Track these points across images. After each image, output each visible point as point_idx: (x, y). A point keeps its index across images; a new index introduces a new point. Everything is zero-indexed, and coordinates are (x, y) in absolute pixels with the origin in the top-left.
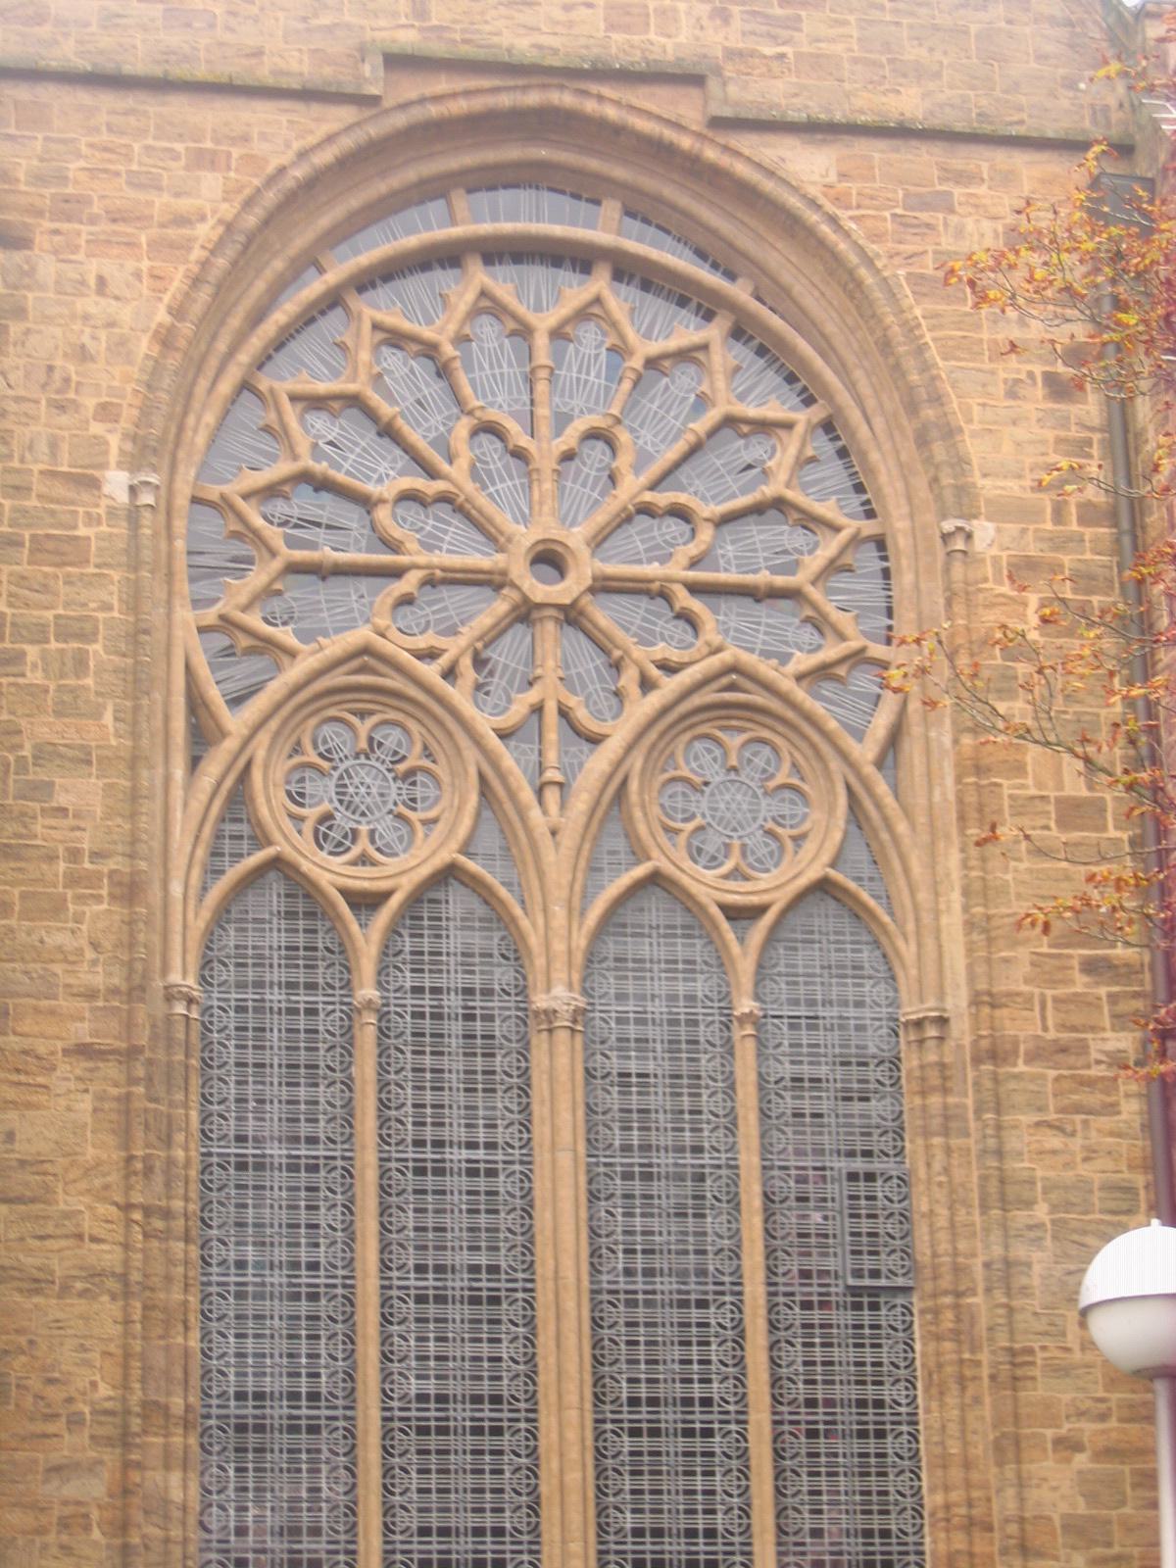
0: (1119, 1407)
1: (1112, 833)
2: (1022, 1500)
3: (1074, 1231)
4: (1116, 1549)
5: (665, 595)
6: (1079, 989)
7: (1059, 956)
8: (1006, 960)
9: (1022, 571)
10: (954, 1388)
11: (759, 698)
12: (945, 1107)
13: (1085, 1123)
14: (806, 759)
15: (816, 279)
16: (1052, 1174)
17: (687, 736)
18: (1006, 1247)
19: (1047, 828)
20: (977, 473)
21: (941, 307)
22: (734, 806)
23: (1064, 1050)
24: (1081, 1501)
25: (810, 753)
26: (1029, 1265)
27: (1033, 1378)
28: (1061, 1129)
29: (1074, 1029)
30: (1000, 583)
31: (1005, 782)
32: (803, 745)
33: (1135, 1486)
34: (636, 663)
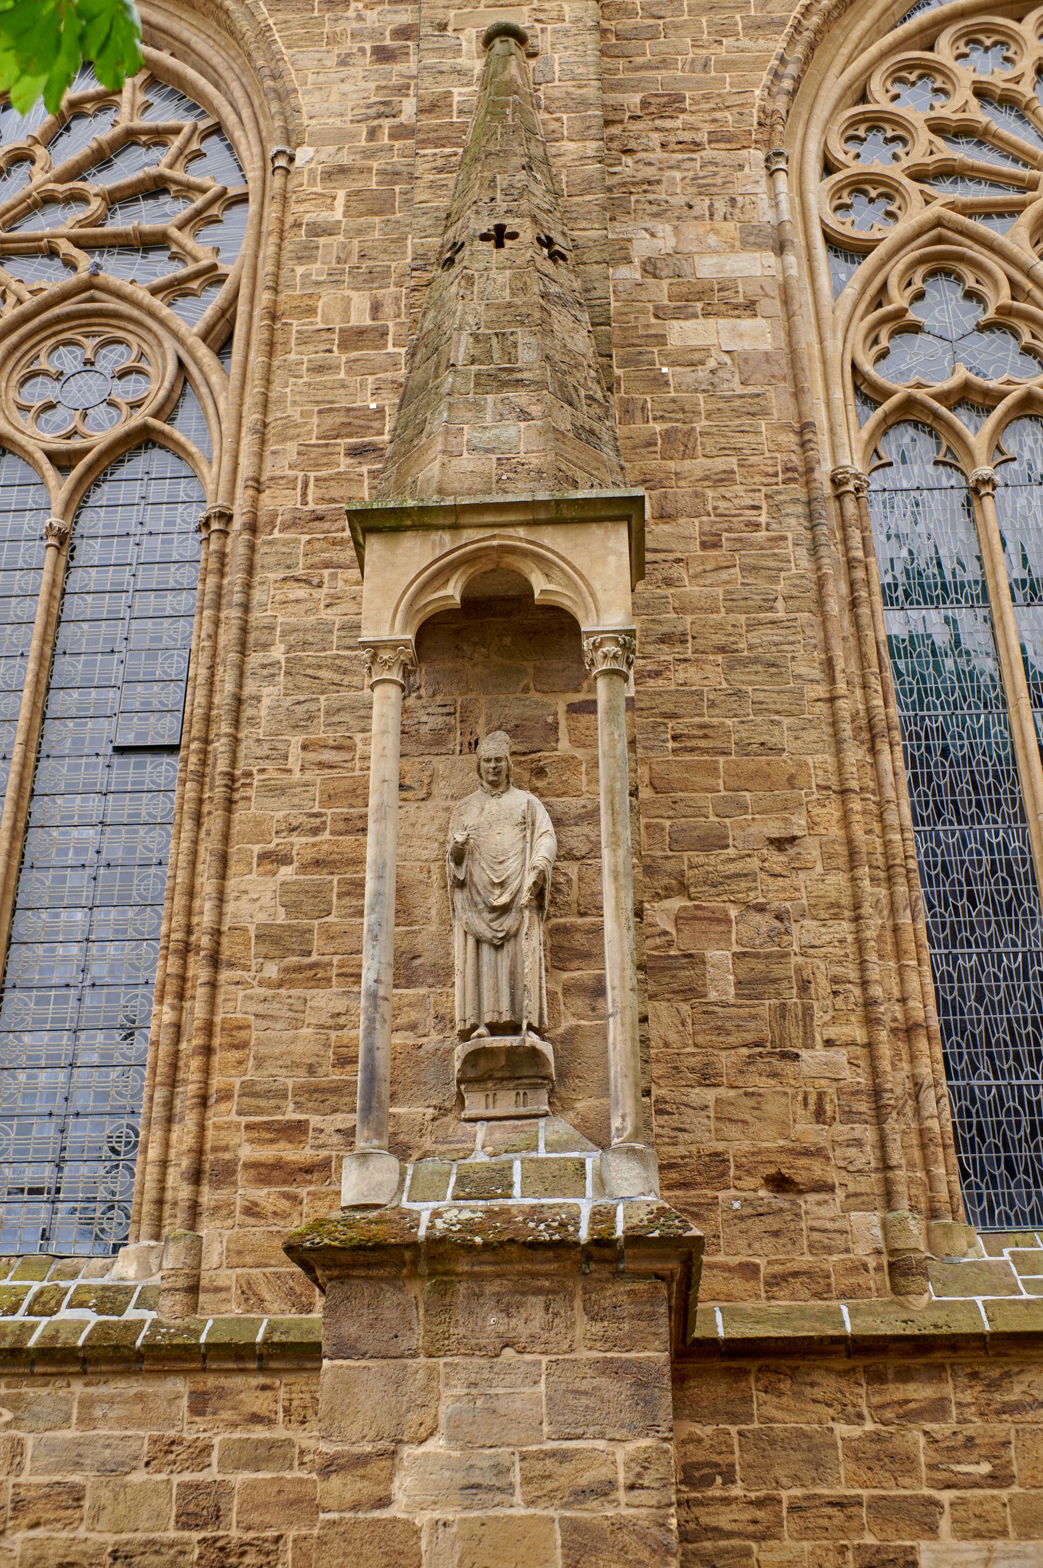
0: (334, 820)
1: (390, 349)
2: (220, 915)
3: (309, 666)
4: (314, 957)
5: (52, 253)
6: (342, 469)
7: (327, 445)
8: (274, 453)
9: (337, 173)
10: (188, 825)
11: (113, 304)
12: (220, 587)
13: (334, 577)
14: (151, 347)
15: (210, 32)
16: (293, 619)
17: (53, 340)
18: (240, 686)
19: (330, 351)
20: (305, 116)
21: (289, 17)
22: (85, 389)
23: (320, 519)
24: (282, 911)
25: (154, 342)
26: (258, 698)
27: (248, 799)
28: (308, 582)
29: (333, 500)
30: (315, 185)
31: (295, 322)
32: (149, 338)
33: (340, 896)
34: (14, 293)
